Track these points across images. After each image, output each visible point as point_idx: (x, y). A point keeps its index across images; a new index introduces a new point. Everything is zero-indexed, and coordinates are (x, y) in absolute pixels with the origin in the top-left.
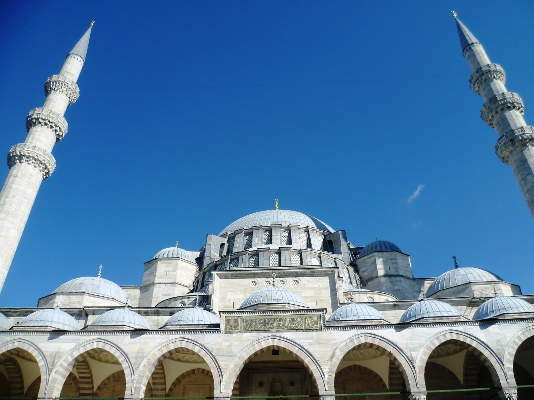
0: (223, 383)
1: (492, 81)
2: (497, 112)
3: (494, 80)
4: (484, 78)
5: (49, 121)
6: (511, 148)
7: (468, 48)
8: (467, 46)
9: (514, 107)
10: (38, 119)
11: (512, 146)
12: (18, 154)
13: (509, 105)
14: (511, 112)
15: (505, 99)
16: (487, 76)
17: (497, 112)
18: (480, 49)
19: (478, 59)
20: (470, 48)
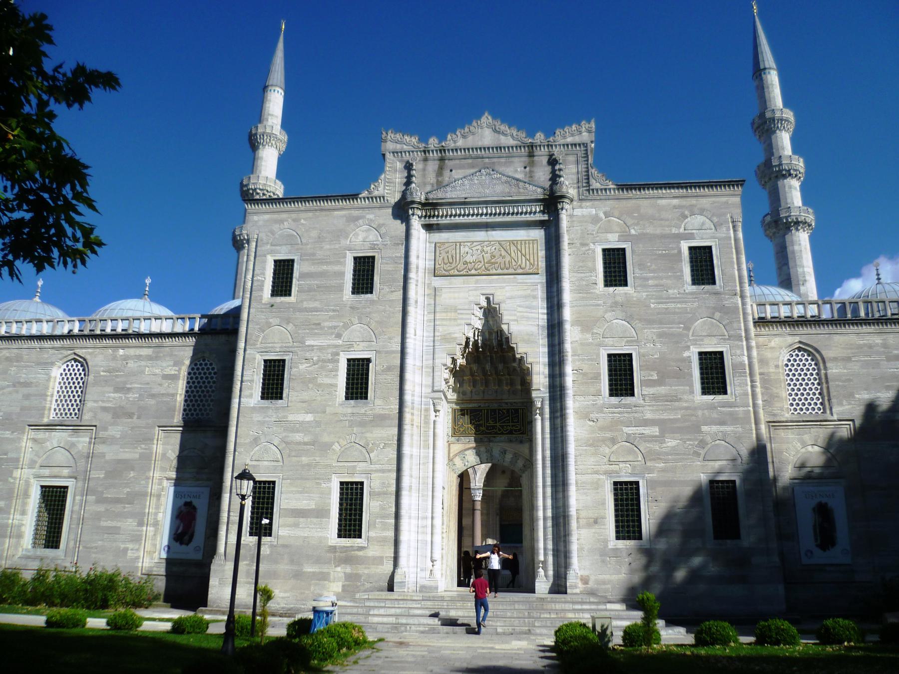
0: (477, 479)
1: (775, 132)
2: (770, 179)
3: (778, 131)
4: (766, 128)
5: (267, 191)
6: (774, 230)
7: (758, 74)
8: (758, 72)
9: (790, 175)
10: (255, 189)
11: (776, 228)
12: (246, 237)
13: (784, 172)
14: (785, 181)
15: (781, 164)
16: (770, 125)
17: (770, 179)
18: (773, 78)
19: (766, 94)
20: (760, 75)
